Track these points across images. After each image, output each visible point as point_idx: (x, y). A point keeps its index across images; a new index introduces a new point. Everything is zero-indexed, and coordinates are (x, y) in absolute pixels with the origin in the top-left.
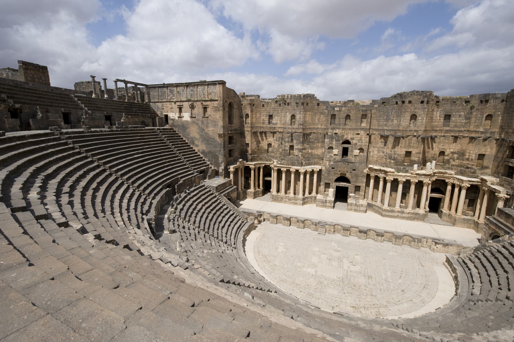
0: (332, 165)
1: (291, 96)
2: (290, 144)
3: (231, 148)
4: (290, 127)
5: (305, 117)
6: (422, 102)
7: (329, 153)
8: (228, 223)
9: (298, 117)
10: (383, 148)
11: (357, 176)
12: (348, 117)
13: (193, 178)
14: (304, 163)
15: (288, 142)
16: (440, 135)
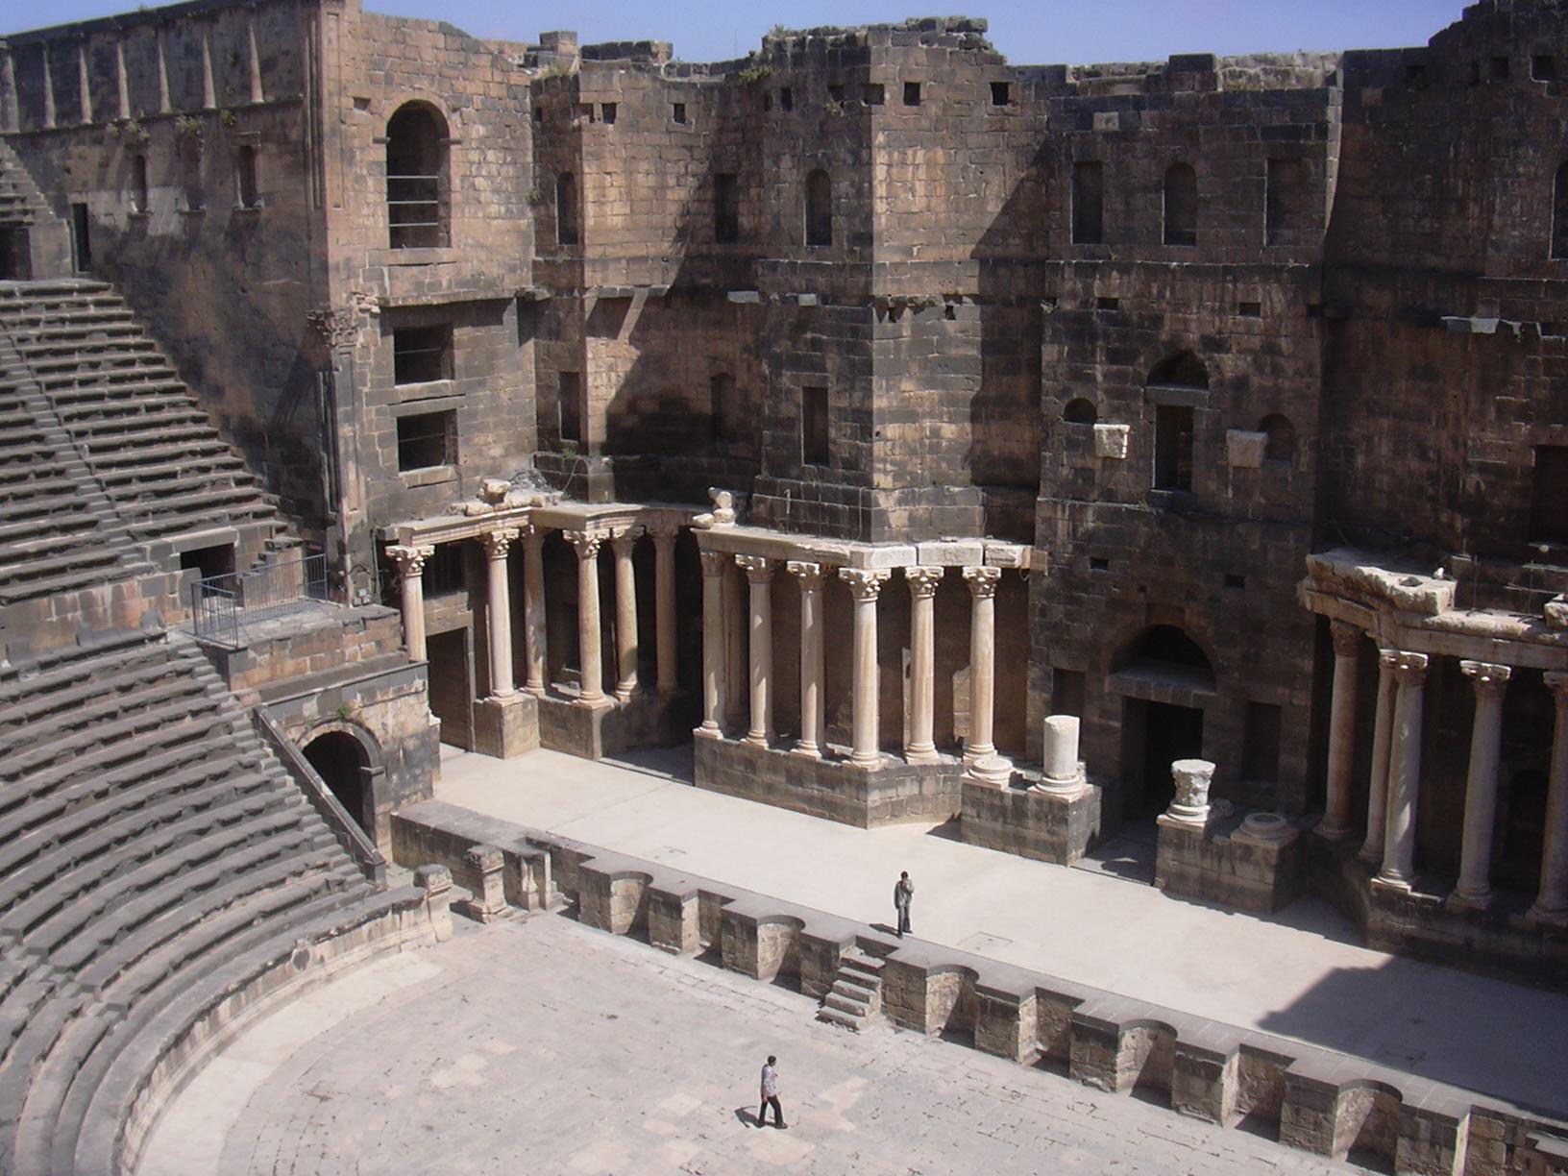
0: (1091, 536)
2: (809, 378)
3: (426, 407)
7: (1072, 445)
8: (204, 874)
12: (1177, 178)
13: (104, 593)
14: (898, 517)
15: (796, 363)
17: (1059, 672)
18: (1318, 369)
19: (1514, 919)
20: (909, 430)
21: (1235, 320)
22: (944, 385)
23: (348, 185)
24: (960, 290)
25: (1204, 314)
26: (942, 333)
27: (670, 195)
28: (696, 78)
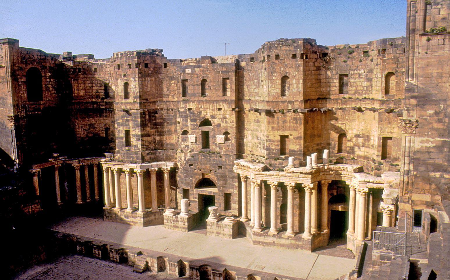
0: (189, 160)
1: (122, 54)
2: (126, 128)
4: (124, 101)
5: (142, 86)
6: (294, 56)
7: (184, 140)
9: (132, 86)
10: (257, 130)
11: (224, 178)
14: (147, 158)
16: (335, 106)
17: (184, 189)
18: (235, 122)
19: (283, 236)
20: (149, 139)
21: (217, 112)
22: (157, 128)
23: (17, 87)
24: (159, 108)
25: (211, 111)
26: (155, 117)
27: (94, 88)
28: (99, 62)
